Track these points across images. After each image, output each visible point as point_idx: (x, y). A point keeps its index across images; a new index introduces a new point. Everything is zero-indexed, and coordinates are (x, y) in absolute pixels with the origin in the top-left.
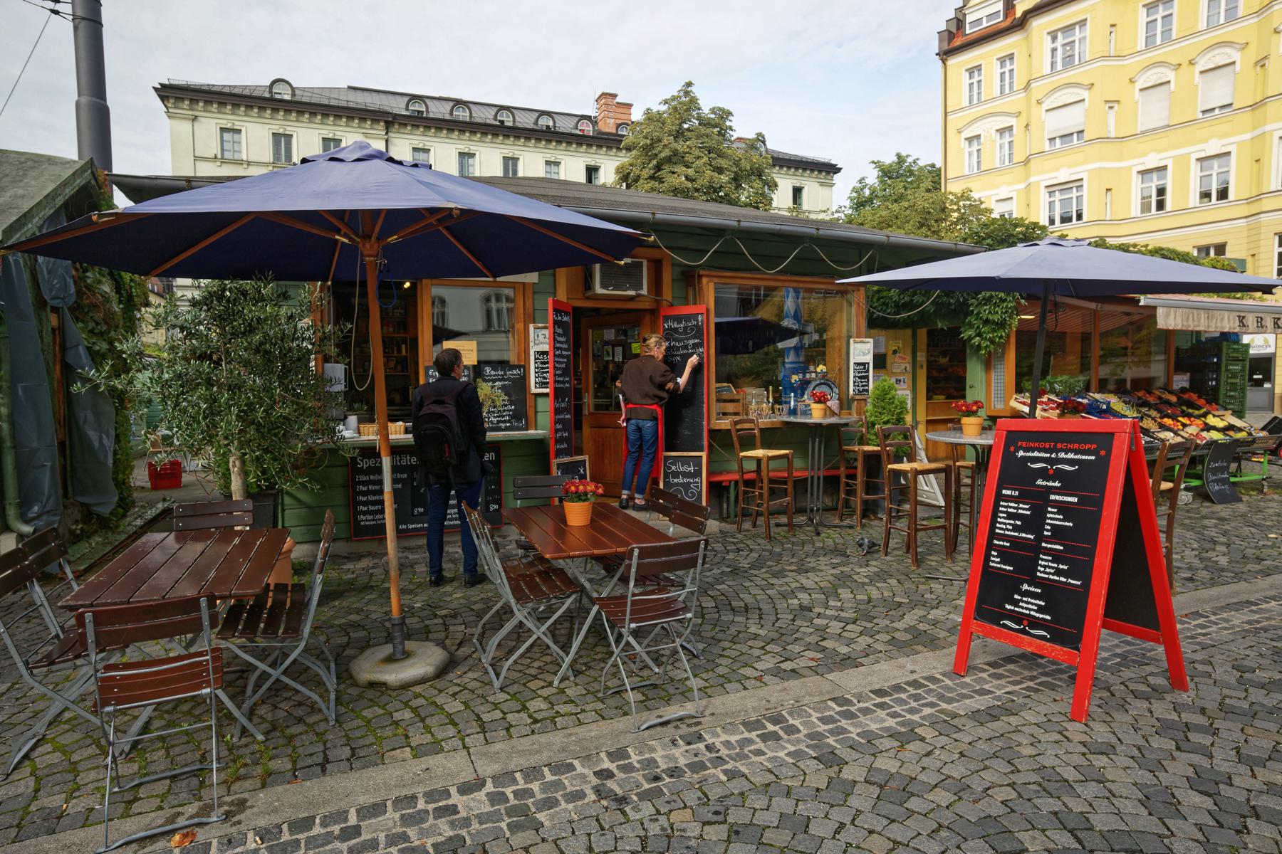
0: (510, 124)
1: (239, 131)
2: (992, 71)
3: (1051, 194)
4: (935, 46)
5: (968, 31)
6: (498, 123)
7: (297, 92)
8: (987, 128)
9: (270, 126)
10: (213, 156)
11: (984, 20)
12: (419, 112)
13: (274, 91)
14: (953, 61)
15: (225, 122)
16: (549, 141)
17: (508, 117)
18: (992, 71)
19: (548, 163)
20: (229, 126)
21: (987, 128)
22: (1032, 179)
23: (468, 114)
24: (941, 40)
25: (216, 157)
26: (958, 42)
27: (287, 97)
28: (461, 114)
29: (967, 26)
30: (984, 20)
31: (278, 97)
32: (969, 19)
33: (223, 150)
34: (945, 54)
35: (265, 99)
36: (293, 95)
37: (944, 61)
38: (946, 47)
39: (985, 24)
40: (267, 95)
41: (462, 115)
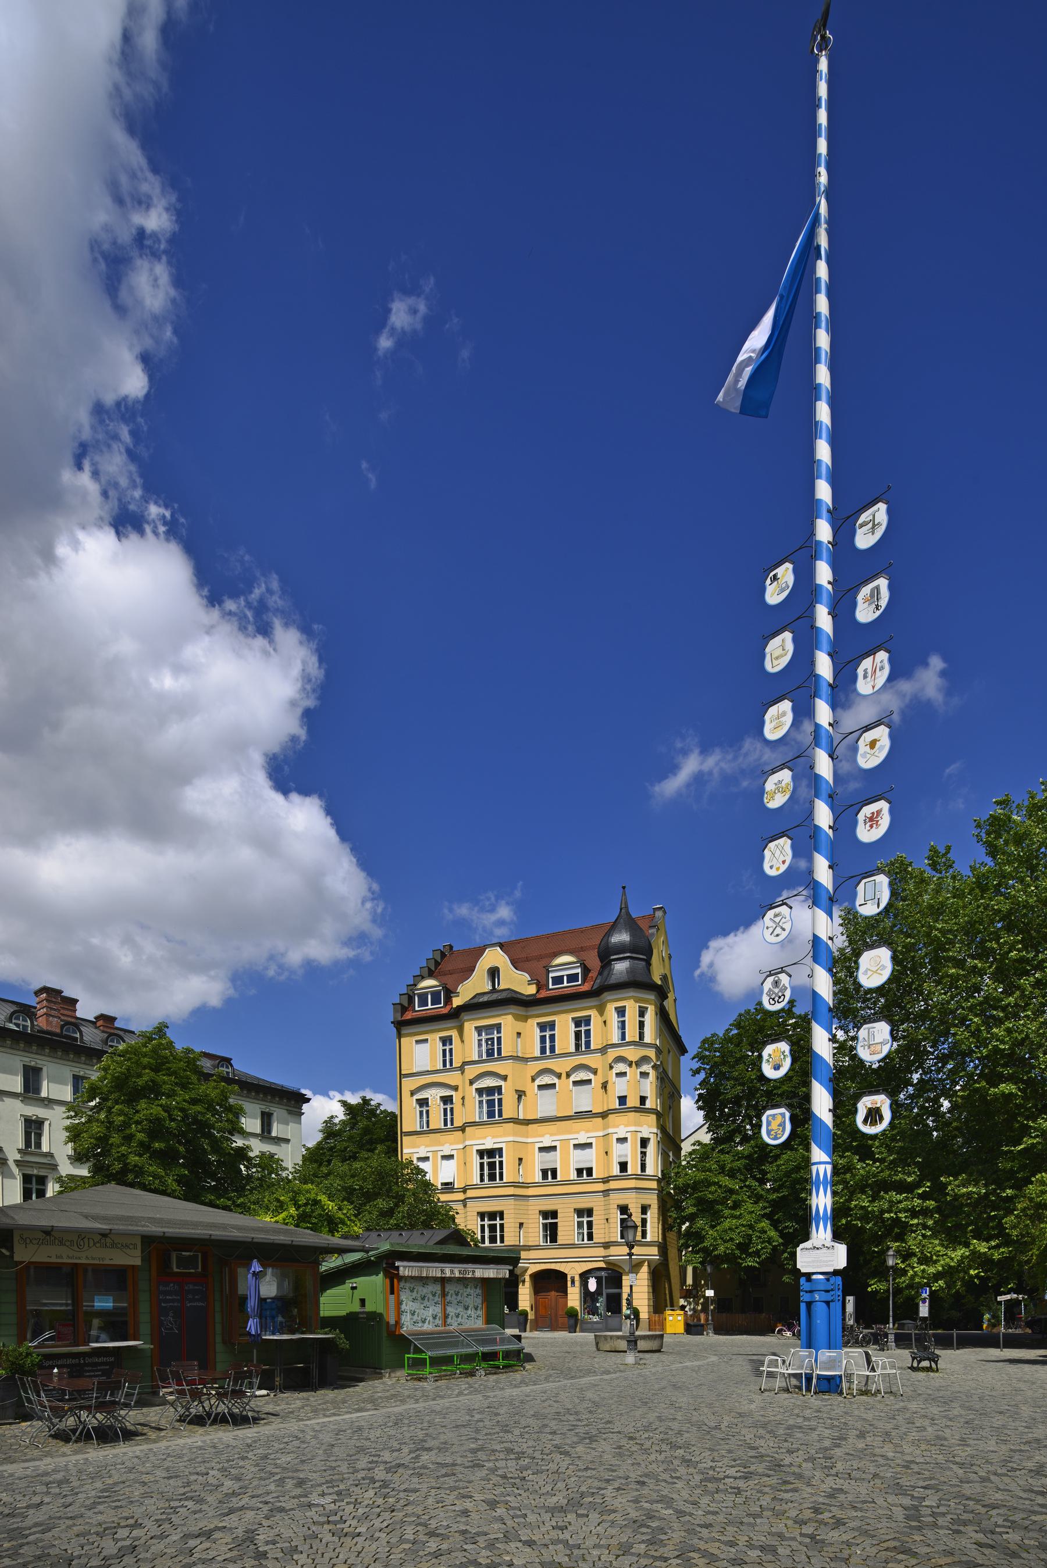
22: (468, 1143)
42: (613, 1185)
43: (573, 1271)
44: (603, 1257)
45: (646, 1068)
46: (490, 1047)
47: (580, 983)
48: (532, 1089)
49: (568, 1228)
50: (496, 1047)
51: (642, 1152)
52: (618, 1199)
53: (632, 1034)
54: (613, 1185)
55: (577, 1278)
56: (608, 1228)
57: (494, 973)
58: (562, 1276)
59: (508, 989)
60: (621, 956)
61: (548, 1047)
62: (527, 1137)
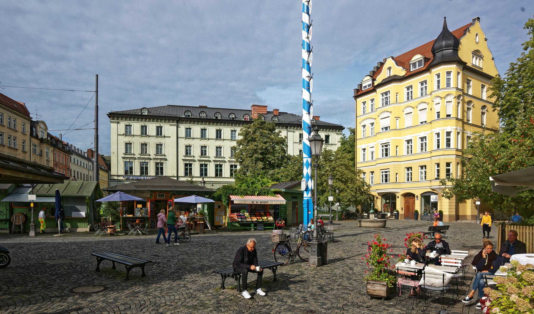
0: (219, 118)
1: (131, 126)
2: (369, 103)
3: (383, 147)
4: (353, 94)
5: (363, 90)
6: (215, 118)
7: (150, 111)
8: (367, 123)
9: (140, 124)
10: (123, 134)
11: (367, 86)
12: (188, 115)
13: (142, 111)
14: (358, 100)
15: (127, 123)
16: (232, 124)
17: (219, 115)
18: (369, 104)
19: (232, 131)
20: (128, 124)
21: (367, 123)
23: (205, 115)
24: (355, 92)
25: (124, 134)
26: (359, 93)
27: (146, 114)
28: (203, 115)
29: (363, 88)
30: (367, 86)
31: (144, 114)
32: (363, 85)
33: (126, 132)
34: (356, 97)
35: (139, 115)
36: (149, 112)
37: (356, 99)
38: (356, 95)
39: (367, 88)
40: (140, 114)
41: (203, 115)
42: (434, 154)
43: (418, 193)
44: (430, 187)
45: (449, 98)
46: (386, 101)
47: (423, 66)
48: (403, 115)
49: (416, 173)
50: (388, 101)
51: (447, 139)
52: (436, 160)
53: (443, 84)
54: (434, 154)
55: (419, 197)
56: (432, 173)
57: (390, 68)
58: (413, 195)
59: (395, 75)
60: (440, 50)
61: (409, 97)
62: (401, 136)
